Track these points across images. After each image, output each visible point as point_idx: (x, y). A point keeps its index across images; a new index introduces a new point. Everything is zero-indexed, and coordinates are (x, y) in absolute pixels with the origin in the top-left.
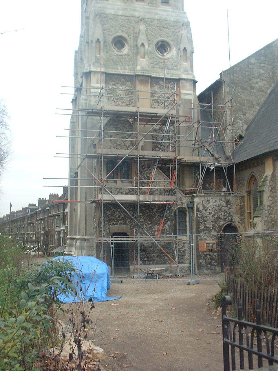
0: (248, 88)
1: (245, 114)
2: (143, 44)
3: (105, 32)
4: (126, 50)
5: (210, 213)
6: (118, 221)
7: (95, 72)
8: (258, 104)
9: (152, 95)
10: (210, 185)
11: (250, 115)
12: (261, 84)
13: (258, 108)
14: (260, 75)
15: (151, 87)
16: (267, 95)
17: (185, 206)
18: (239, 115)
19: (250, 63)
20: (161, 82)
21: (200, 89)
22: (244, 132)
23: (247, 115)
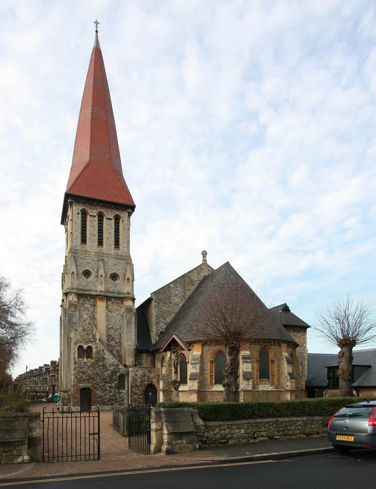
0: (168, 303)
1: (165, 319)
2: (101, 275)
3: (78, 267)
4: (91, 278)
5: (139, 377)
6: (85, 381)
7: (71, 293)
8: (174, 313)
9: (107, 307)
10: (142, 361)
11: (169, 319)
12: (176, 300)
13: (173, 315)
14: (176, 295)
15: (107, 302)
16: (180, 308)
17: (125, 373)
18: (162, 319)
19: (170, 287)
20: (113, 300)
21: (137, 304)
22: (164, 330)
23: (167, 319)
